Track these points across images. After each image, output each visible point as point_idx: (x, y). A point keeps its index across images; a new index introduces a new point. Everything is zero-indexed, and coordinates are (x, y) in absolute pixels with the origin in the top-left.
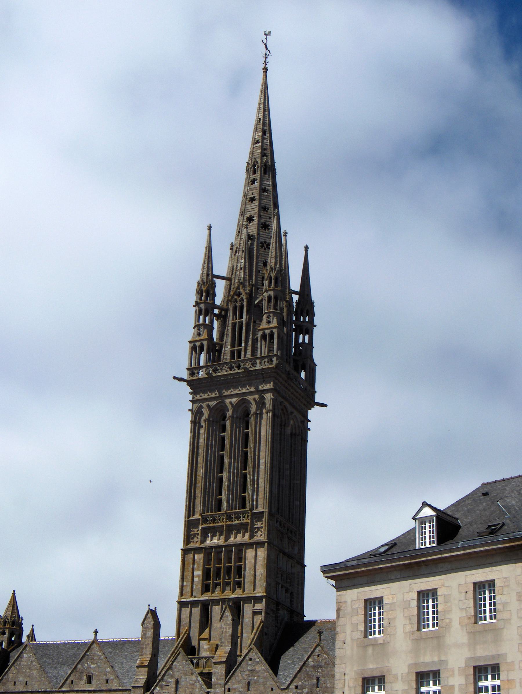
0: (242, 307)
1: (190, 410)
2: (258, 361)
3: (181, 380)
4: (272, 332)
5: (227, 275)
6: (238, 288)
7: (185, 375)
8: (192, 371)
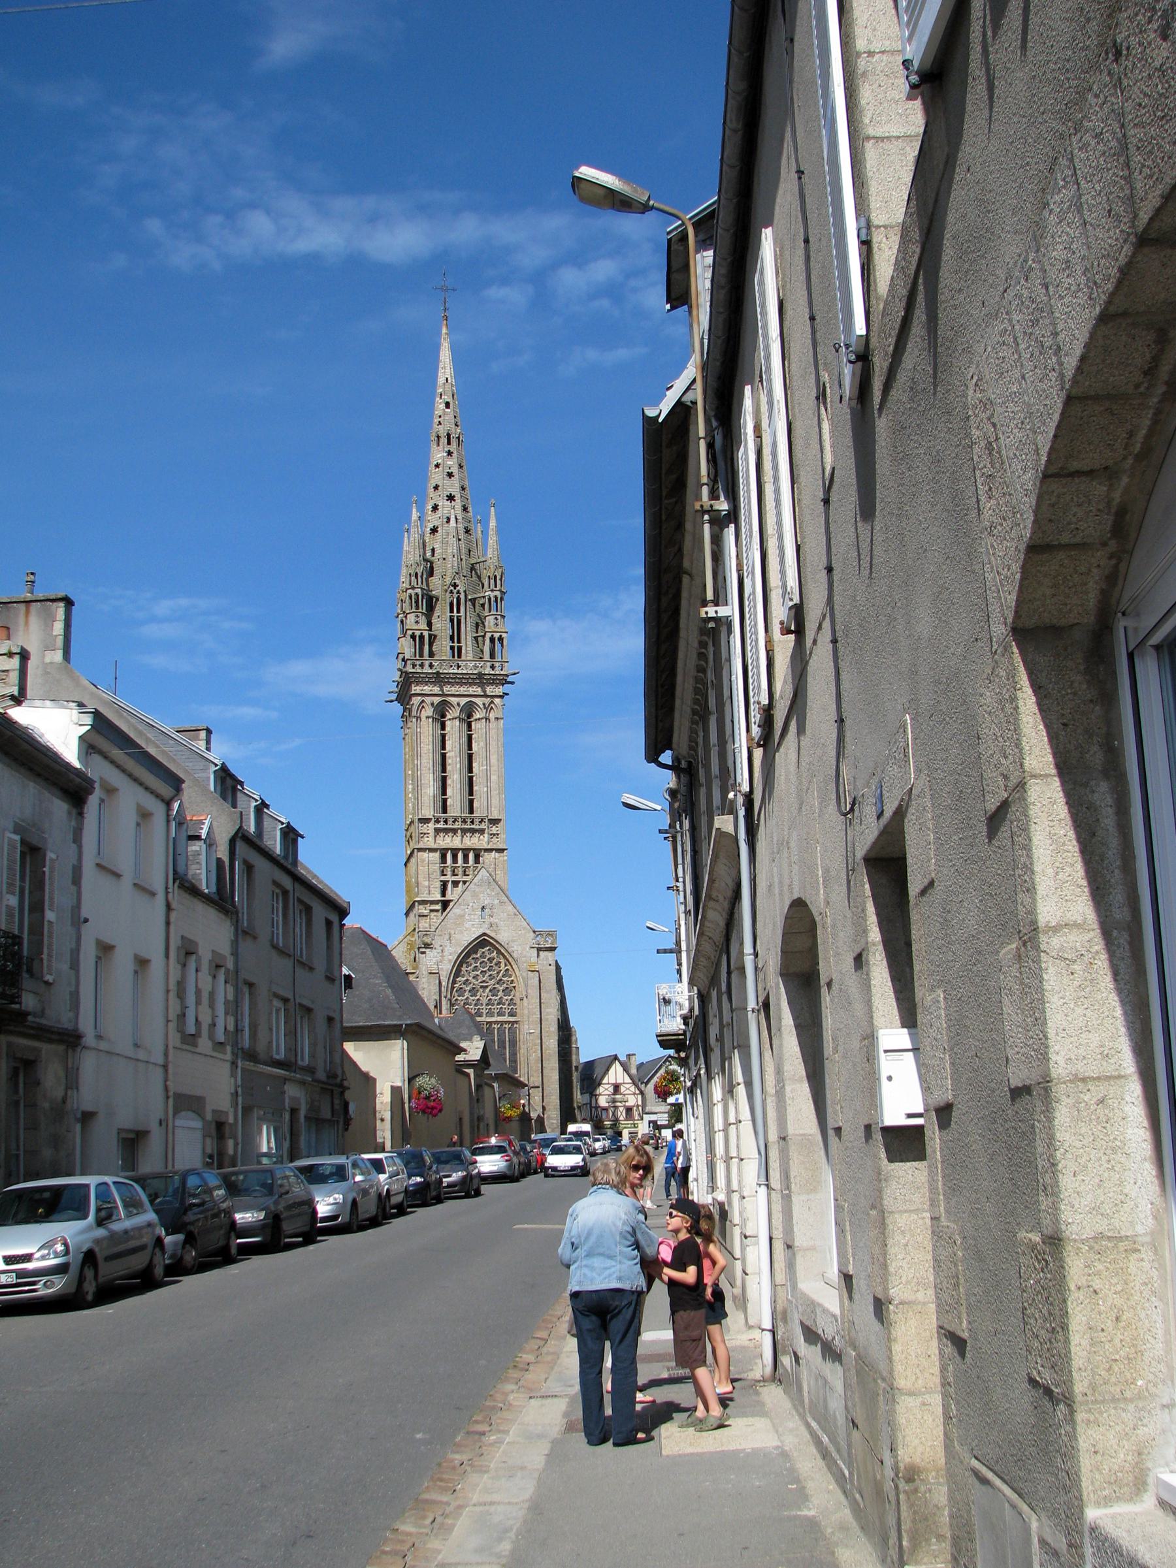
6: (454, 579)
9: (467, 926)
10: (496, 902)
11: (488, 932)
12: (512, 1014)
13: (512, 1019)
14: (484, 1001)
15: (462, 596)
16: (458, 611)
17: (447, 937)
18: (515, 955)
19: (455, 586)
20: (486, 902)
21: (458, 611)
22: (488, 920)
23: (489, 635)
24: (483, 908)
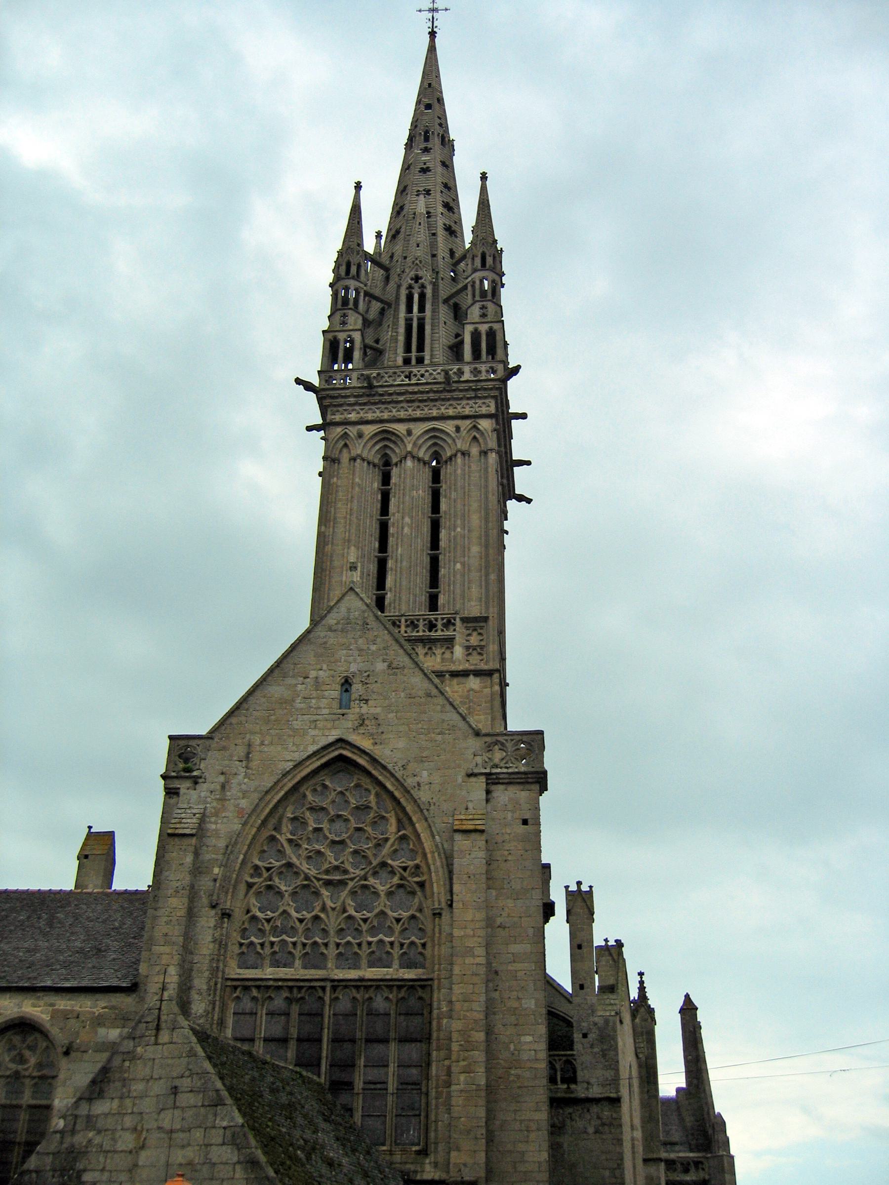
3: (308, 387)
9: (297, 724)
10: (381, 666)
11: (353, 738)
12: (409, 964)
13: (409, 974)
14: (333, 922)
15: (429, 291)
16: (422, 309)
17: (241, 751)
18: (423, 796)
19: (417, 279)
20: (353, 668)
21: (422, 309)
22: (356, 709)
23: (469, 329)
24: (346, 684)
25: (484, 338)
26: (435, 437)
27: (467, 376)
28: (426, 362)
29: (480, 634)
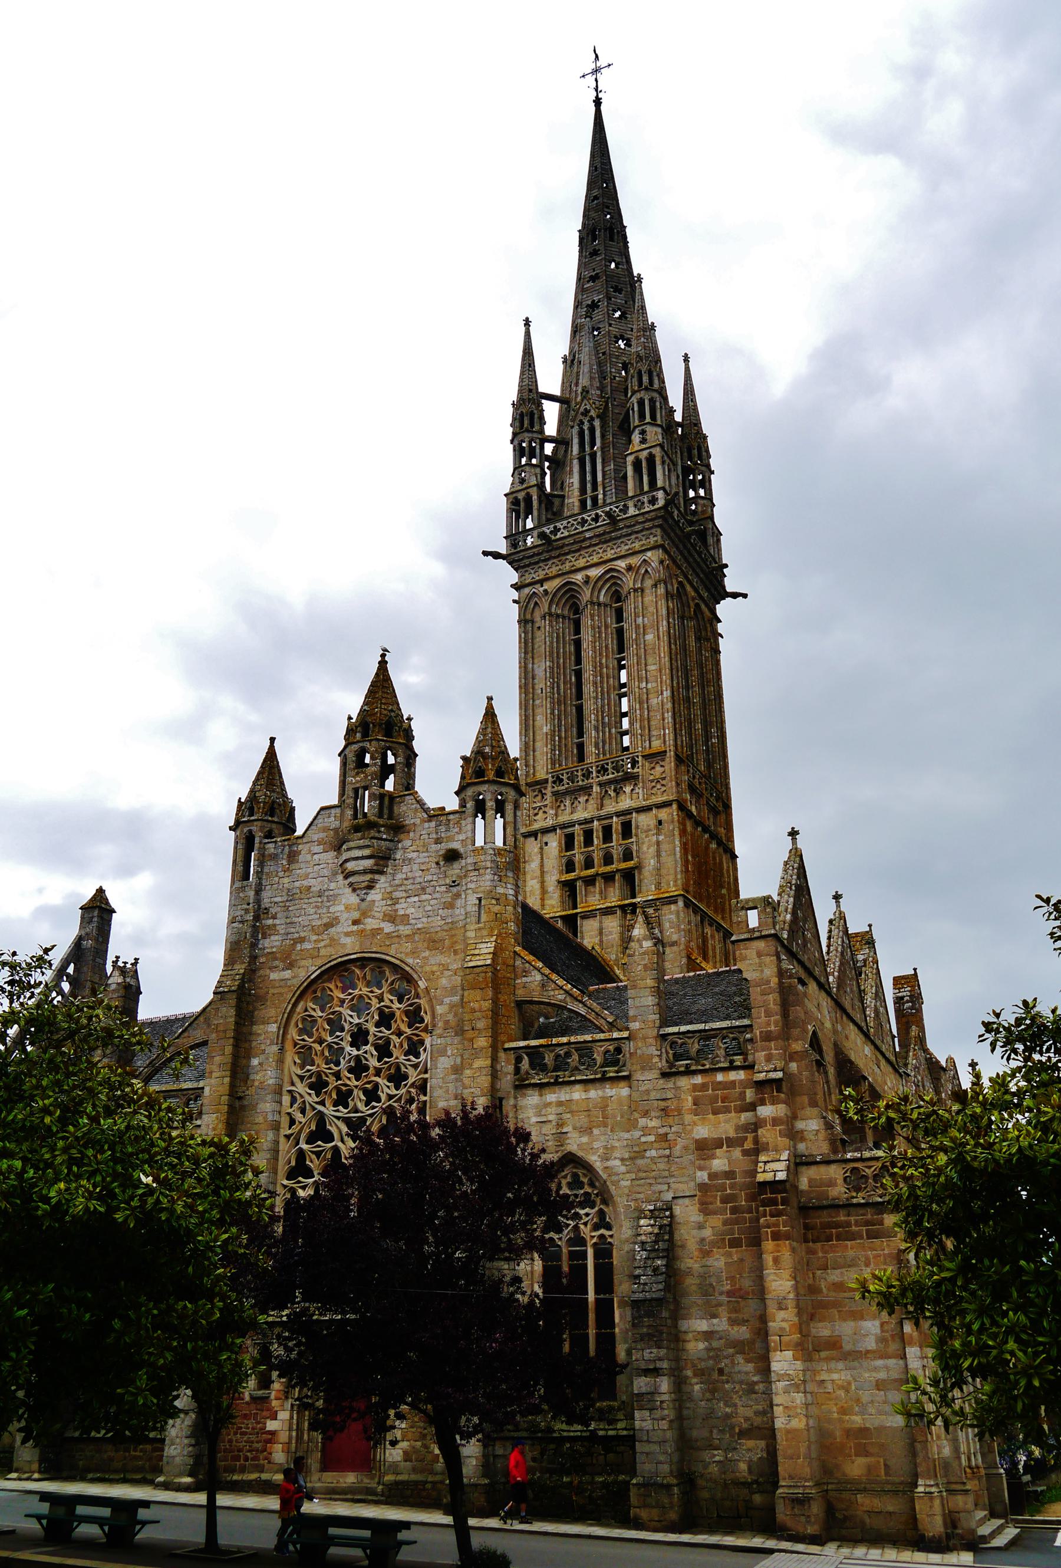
0: (592, 430)
1: (515, 601)
2: (630, 504)
3: (496, 555)
4: (650, 454)
5: (562, 391)
7: (502, 548)
8: (513, 538)
23: (630, 459)
25: (644, 464)
26: (613, 577)
27: (632, 511)
28: (600, 502)
29: (662, 766)
